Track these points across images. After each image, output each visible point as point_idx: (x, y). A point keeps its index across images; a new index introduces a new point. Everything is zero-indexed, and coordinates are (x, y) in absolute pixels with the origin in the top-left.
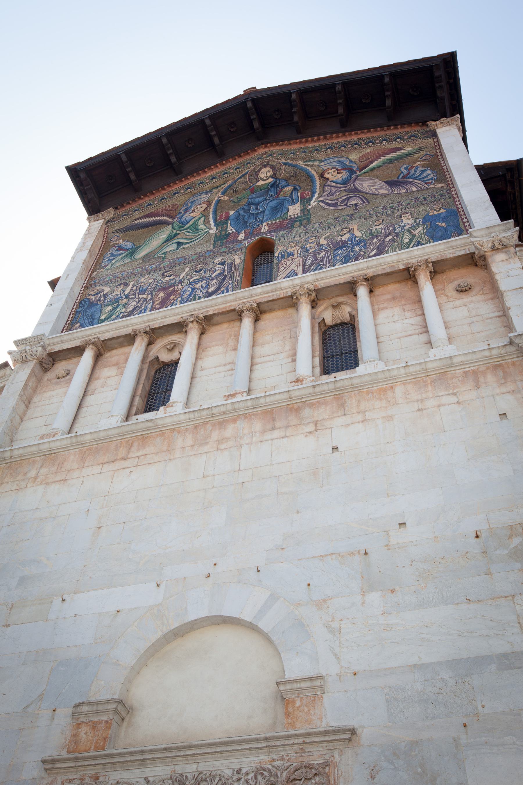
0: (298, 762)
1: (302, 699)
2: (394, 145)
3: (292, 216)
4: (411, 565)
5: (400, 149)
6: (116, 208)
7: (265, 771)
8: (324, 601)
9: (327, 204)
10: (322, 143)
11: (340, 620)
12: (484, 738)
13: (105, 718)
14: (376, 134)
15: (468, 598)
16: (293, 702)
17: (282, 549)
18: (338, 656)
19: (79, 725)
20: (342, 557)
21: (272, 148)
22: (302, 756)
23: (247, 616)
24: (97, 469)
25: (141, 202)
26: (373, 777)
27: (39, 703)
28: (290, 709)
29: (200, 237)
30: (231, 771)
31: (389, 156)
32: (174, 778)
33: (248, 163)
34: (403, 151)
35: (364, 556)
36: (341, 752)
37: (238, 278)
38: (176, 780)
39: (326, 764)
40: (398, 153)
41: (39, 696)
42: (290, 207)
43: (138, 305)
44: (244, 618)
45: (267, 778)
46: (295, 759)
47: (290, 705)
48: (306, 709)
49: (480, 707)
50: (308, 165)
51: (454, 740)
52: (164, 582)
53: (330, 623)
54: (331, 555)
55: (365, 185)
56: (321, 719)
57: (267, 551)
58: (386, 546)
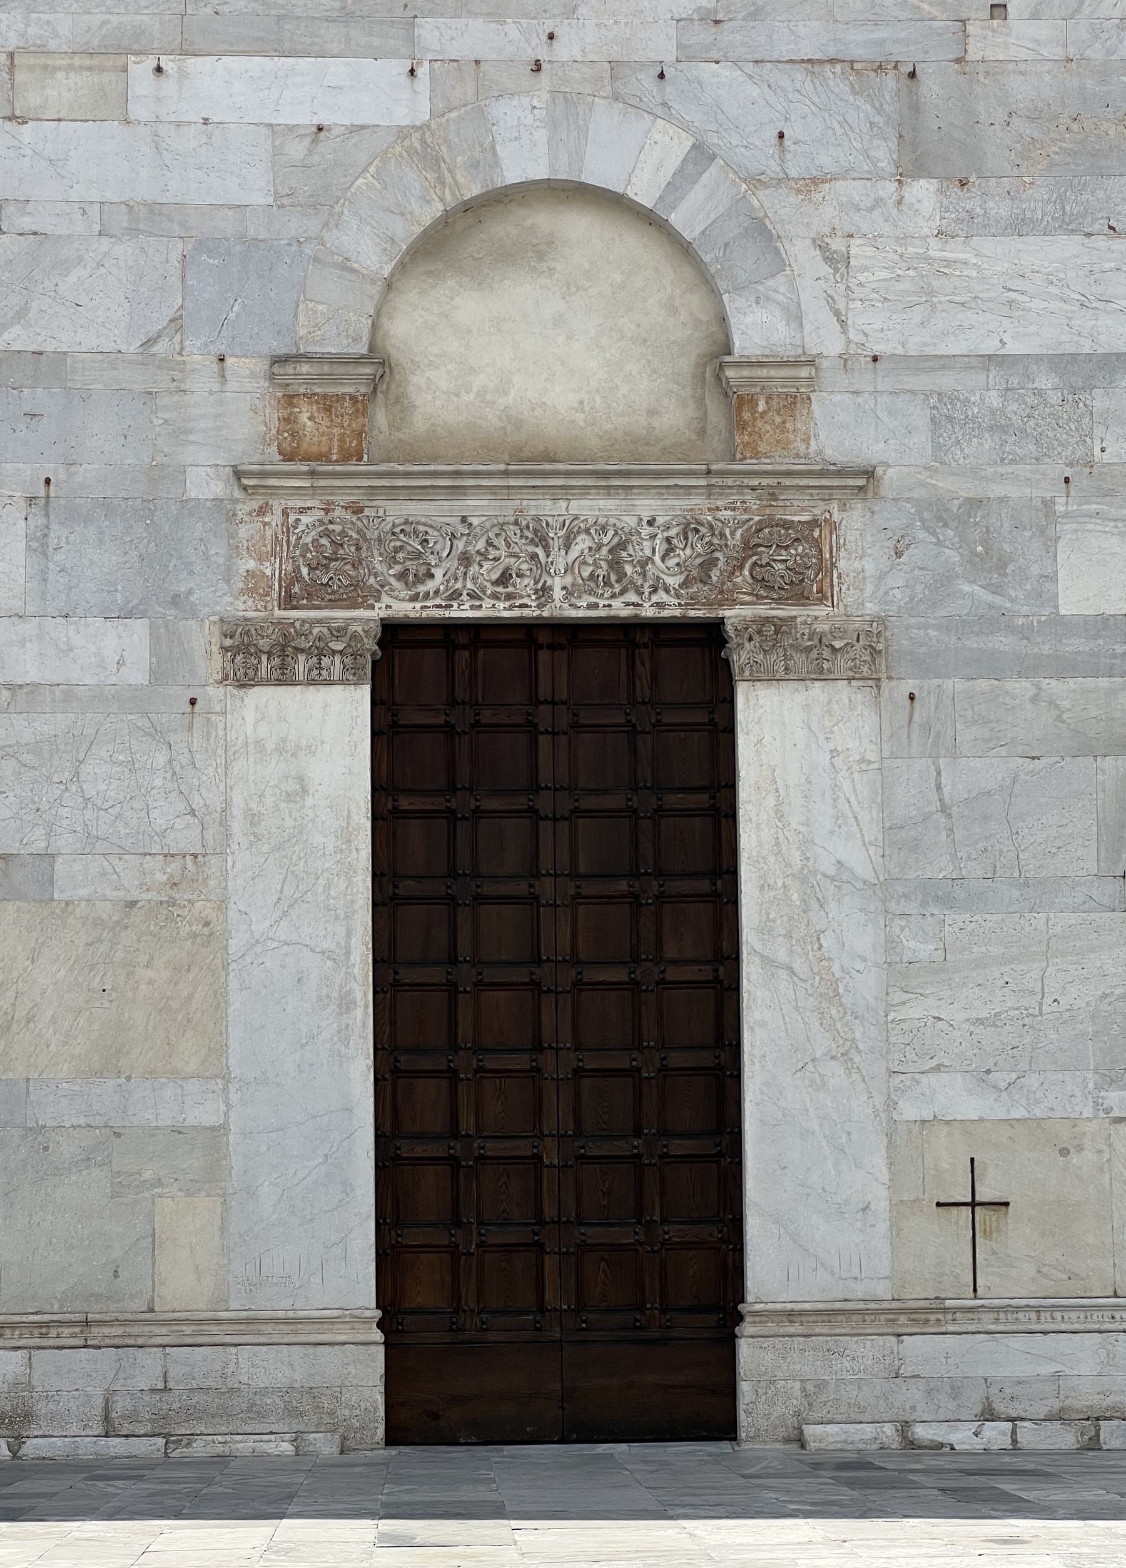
0: (763, 516)
1: (769, 399)
4: (1008, 124)
7: (702, 525)
8: (816, 182)
11: (849, 236)
12: (1094, 506)
13: (349, 390)
15: (1113, 223)
16: (753, 401)
17: (717, 22)
18: (843, 318)
19: (290, 399)
20: (858, 72)
22: (771, 506)
23: (644, 193)
26: (899, 554)
27: (178, 337)
28: (746, 415)
30: (635, 520)
32: (524, 523)
35: (908, 81)
36: (843, 508)
38: (528, 527)
39: (814, 523)
41: (172, 321)
44: (635, 198)
45: (707, 539)
46: (758, 509)
47: (746, 408)
48: (778, 420)
49: (1097, 450)
51: (1045, 502)
52: (426, 64)
53: (827, 240)
54: (832, 61)
56: (807, 441)
57: (678, 21)
58: (958, 61)
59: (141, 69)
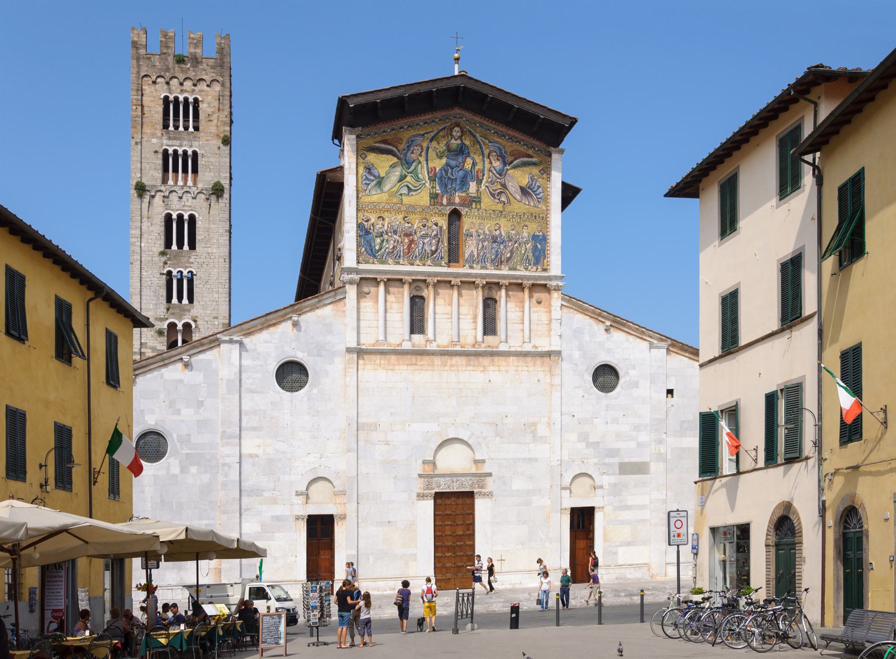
2: (530, 152)
3: (471, 193)
5: (531, 157)
6: (363, 127)
9: (490, 192)
10: (493, 126)
14: (523, 138)
21: (463, 112)
24: (405, 367)
25: (379, 126)
29: (421, 188)
31: (525, 159)
33: (448, 118)
34: (532, 159)
37: (446, 245)
40: (530, 159)
42: (471, 183)
43: (395, 244)
50: (482, 140)
55: (510, 184)
59: (407, 424)
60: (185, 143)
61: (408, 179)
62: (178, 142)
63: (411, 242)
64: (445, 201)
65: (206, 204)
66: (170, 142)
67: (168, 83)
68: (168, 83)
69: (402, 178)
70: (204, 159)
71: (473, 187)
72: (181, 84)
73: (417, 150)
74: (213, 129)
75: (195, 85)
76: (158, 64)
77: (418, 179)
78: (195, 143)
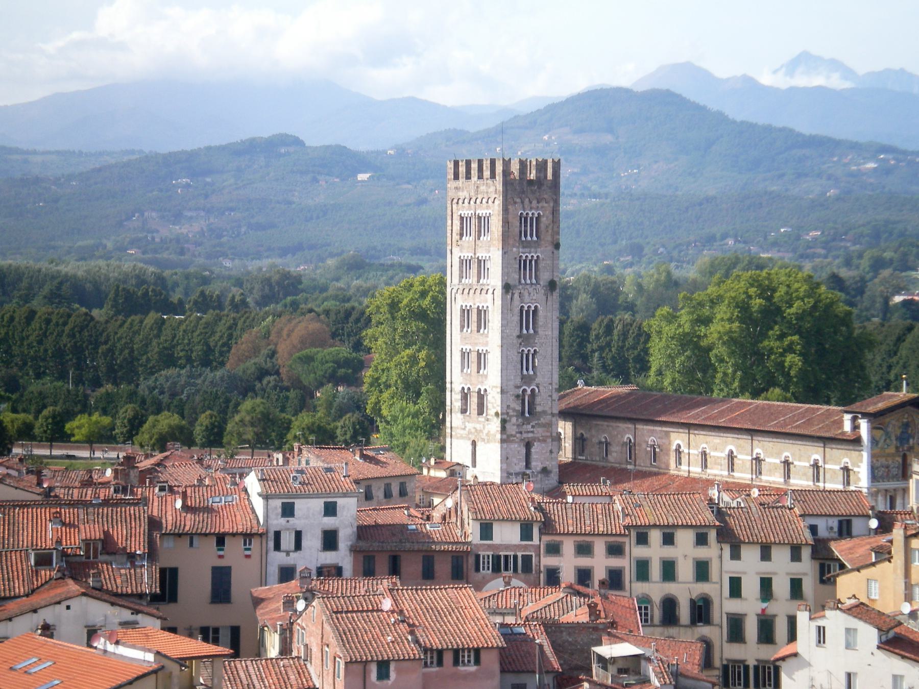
60: (533, 250)
61: (888, 441)
62: (528, 250)
63: (889, 471)
64: (901, 450)
65: (544, 298)
66: (524, 250)
67: (522, 202)
68: (522, 202)
69: (885, 440)
70: (544, 262)
71: (911, 441)
72: (531, 202)
73: (891, 426)
74: (549, 238)
75: (538, 202)
76: (518, 188)
77: (891, 440)
78: (539, 250)
